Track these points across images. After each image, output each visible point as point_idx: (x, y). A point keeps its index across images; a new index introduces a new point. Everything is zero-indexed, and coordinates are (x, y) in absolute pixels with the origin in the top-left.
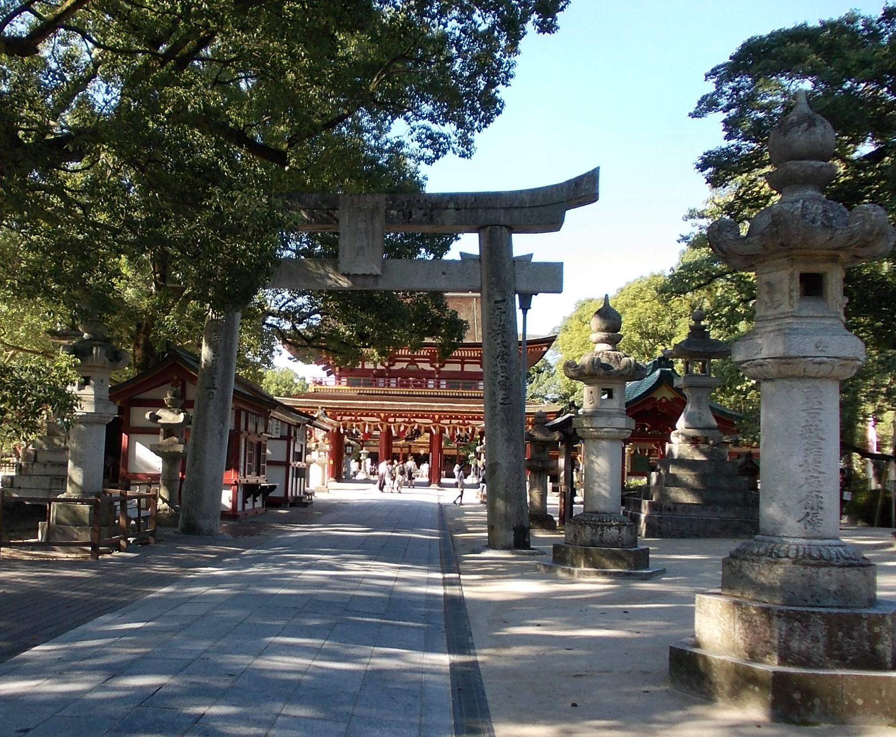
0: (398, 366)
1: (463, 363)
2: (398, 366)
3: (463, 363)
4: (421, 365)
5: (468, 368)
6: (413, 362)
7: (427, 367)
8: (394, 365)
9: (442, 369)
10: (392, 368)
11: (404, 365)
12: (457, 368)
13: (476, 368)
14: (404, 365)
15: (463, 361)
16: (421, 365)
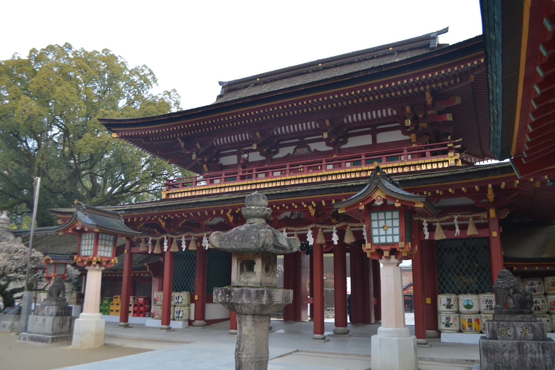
0: (283, 152)
1: (374, 133)
2: (283, 152)
3: (374, 133)
4: (314, 146)
5: (383, 138)
6: (303, 144)
7: (322, 147)
8: (277, 152)
9: (343, 147)
10: (276, 157)
11: (290, 150)
12: (367, 140)
13: (397, 136)
14: (290, 150)
15: (373, 128)
16: (314, 146)
